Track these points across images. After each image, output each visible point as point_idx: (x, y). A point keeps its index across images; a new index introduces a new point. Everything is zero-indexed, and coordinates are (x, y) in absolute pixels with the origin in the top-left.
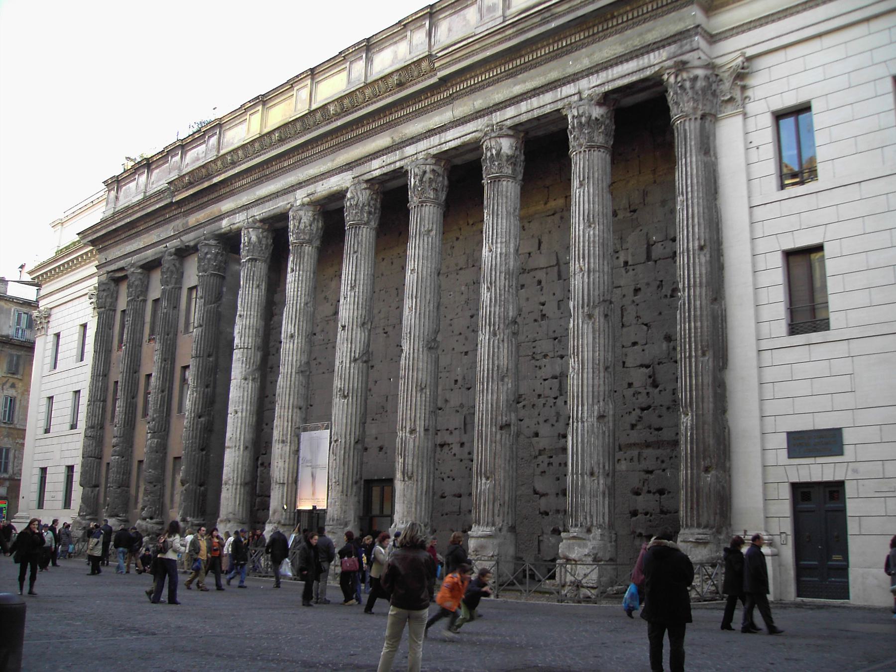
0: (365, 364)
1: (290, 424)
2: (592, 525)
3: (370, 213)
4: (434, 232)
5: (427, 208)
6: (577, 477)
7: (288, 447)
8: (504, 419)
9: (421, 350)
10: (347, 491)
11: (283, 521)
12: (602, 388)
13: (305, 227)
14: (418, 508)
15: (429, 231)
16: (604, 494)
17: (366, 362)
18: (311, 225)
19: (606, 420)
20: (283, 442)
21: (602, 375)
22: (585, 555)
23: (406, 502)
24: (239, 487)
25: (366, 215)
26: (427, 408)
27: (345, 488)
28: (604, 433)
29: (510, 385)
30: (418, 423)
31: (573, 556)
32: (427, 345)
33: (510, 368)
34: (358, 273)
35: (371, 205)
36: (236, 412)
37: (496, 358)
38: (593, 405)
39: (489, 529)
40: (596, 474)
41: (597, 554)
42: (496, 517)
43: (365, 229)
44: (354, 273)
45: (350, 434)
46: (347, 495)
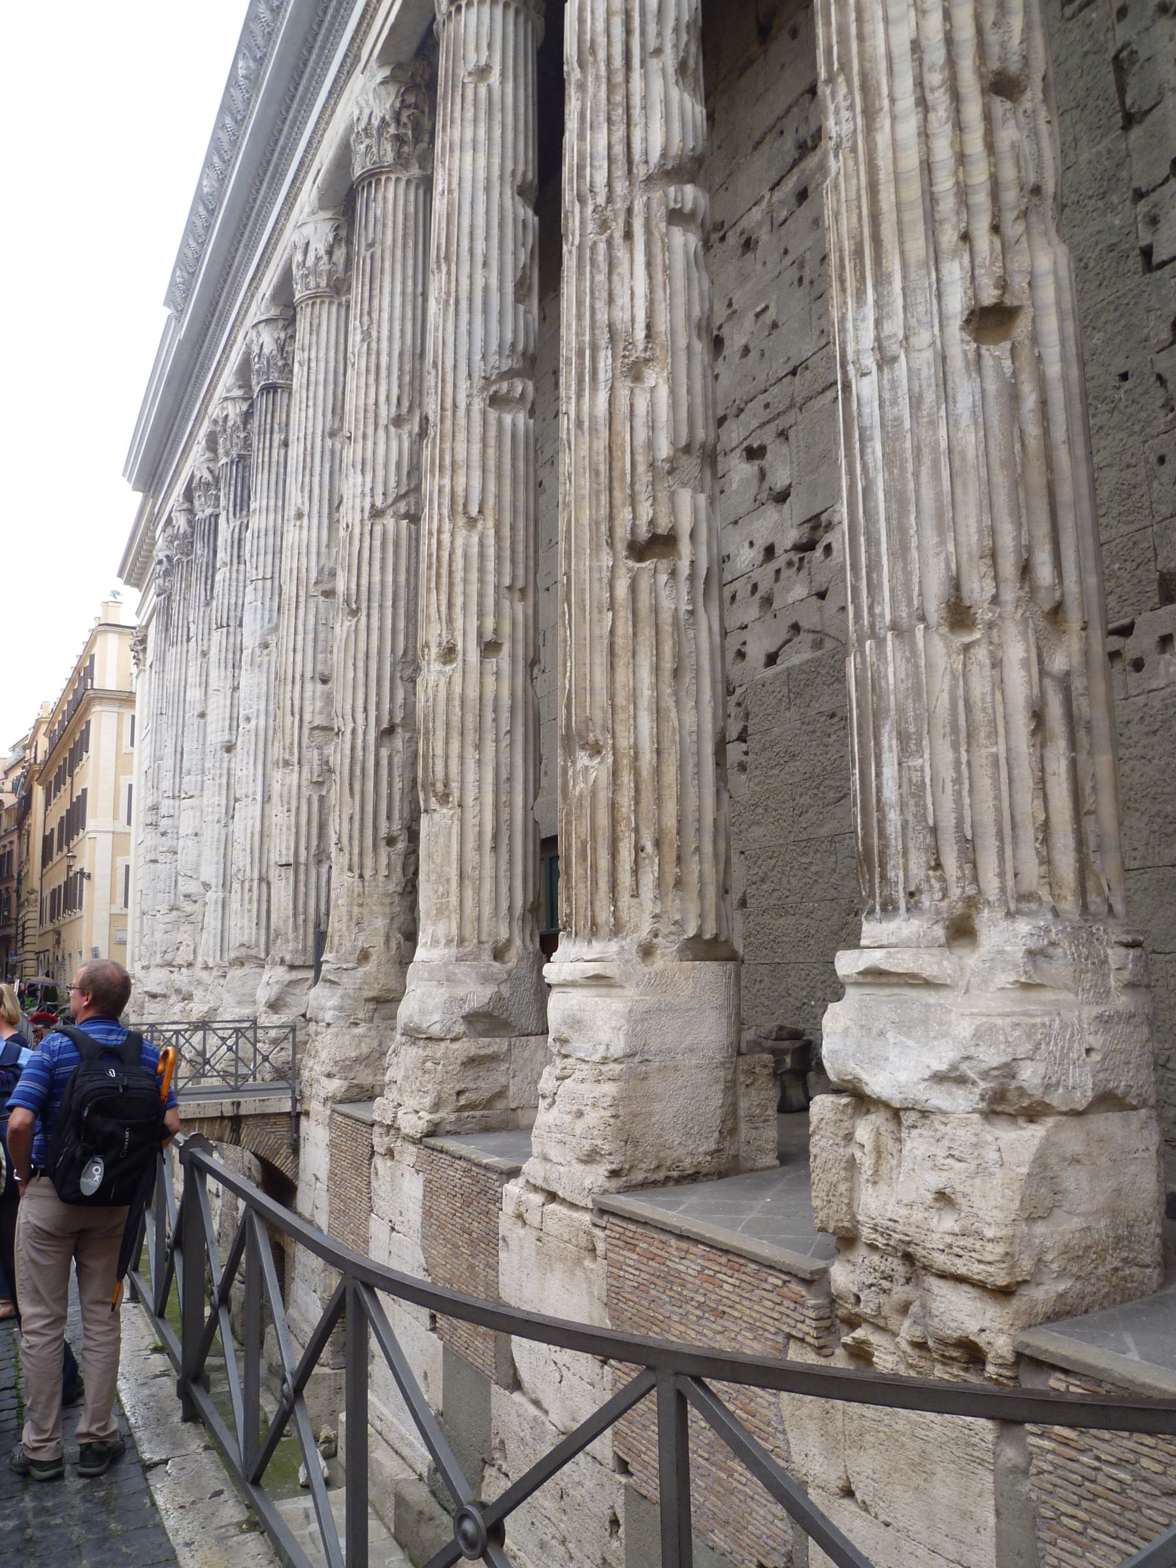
0: (404, 523)
1: (297, 717)
2: (972, 903)
3: (399, 139)
4: (495, 78)
5: (474, 11)
6: (880, 643)
7: (295, 775)
8: (645, 511)
9: (462, 406)
10: (361, 867)
11: (288, 958)
12: (979, 175)
13: (318, 259)
14: (469, 893)
15: (482, 72)
16: (1038, 716)
17: (407, 516)
18: (330, 253)
19: (1022, 327)
20: (287, 763)
21: (973, 110)
22: (939, 1078)
23: (433, 878)
24: (255, 883)
25: (388, 147)
26: (491, 578)
27: (356, 858)
28: (1014, 397)
29: (663, 392)
30: (459, 624)
31: (877, 1084)
32: (484, 388)
33: (662, 326)
34: (376, 292)
35: (404, 119)
36: (248, 719)
37: (601, 305)
38: (936, 256)
39: (598, 948)
40: (984, 614)
41: (1008, 1070)
42: (625, 900)
43: (391, 186)
44: (367, 295)
45: (366, 710)
46: (361, 876)
